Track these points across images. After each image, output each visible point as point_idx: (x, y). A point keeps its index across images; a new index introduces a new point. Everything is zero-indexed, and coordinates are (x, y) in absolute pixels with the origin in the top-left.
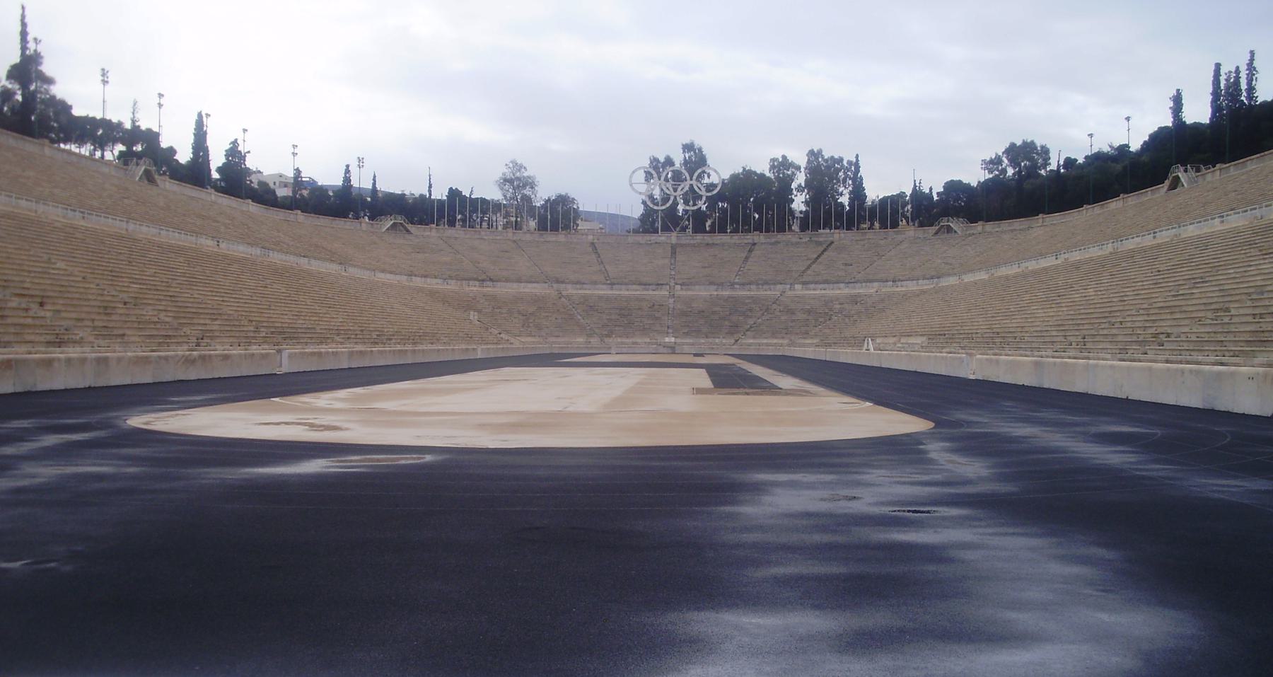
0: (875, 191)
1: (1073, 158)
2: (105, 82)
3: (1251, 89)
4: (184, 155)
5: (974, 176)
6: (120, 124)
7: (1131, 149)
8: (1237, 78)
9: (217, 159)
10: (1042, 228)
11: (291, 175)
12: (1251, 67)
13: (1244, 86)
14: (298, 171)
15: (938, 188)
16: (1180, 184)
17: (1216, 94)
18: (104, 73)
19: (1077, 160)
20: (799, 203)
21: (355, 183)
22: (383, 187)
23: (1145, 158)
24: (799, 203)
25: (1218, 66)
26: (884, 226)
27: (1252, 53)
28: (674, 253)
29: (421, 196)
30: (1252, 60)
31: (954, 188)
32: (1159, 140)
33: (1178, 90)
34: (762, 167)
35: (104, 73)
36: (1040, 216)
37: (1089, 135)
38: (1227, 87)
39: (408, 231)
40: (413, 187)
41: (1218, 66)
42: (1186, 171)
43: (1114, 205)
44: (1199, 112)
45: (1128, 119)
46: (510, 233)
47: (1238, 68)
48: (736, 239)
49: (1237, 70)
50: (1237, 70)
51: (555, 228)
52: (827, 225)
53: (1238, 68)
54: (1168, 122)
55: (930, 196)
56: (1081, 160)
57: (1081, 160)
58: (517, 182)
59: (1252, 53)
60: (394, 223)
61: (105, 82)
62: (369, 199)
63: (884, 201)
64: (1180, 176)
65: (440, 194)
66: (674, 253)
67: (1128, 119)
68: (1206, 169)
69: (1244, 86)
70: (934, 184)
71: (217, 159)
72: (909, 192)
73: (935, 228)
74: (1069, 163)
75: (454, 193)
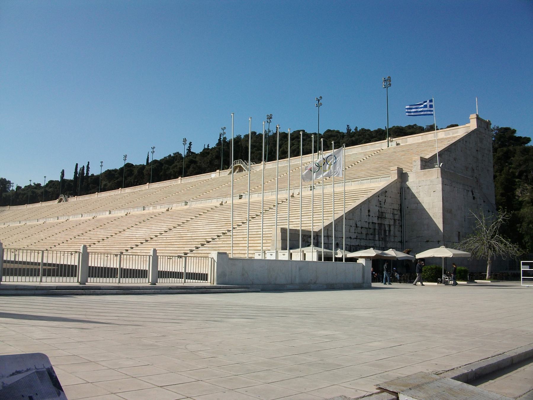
1: (20, 186)
3: (87, 173)
7: (41, 185)
10: (9, 211)
13: (85, 172)
16: (62, 201)
17: (76, 172)
19: (21, 187)
25: (77, 164)
27: (89, 162)
30: (88, 164)
33: (63, 170)
36: (9, 206)
37: (30, 180)
38: (80, 173)
41: (77, 164)
42: (65, 197)
45: (45, 177)
47: (84, 166)
53: (84, 166)
54: (59, 180)
56: (23, 187)
57: (23, 187)
59: (89, 162)
64: (63, 198)
67: (45, 177)
68: (72, 197)
69: (85, 172)
74: (19, 188)
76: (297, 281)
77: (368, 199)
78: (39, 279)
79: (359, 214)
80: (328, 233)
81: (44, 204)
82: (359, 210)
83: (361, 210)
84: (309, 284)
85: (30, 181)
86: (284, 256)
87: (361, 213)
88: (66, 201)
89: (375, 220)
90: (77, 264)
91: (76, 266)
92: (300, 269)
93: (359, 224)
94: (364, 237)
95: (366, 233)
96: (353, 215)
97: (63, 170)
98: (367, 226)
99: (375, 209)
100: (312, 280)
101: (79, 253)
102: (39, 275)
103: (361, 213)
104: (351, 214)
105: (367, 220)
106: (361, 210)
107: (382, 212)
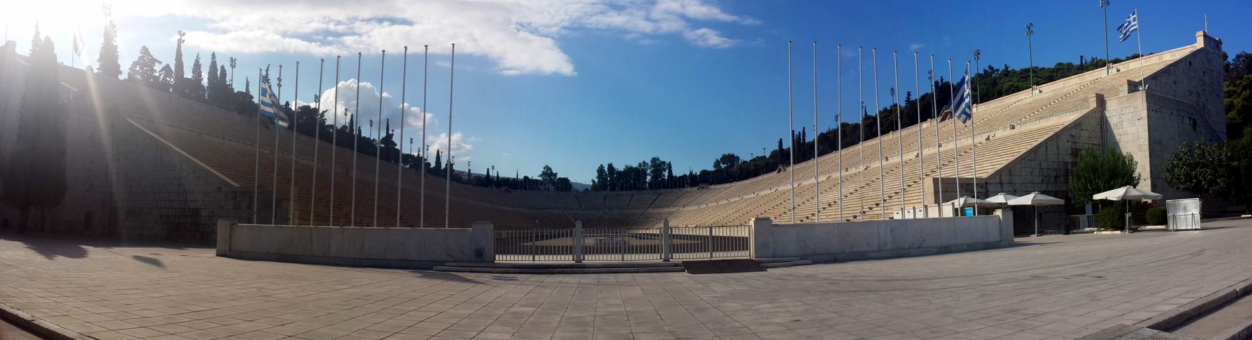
0: (677, 172)
2: (411, 143)
3: (804, 139)
4: (433, 165)
5: (711, 168)
6: (414, 155)
8: (800, 135)
9: (443, 166)
11: (467, 171)
12: (804, 133)
14: (469, 170)
15: (698, 173)
18: (411, 139)
20: (649, 178)
21: (491, 174)
22: (501, 175)
23: (771, 161)
24: (649, 178)
26: (679, 187)
27: (804, 128)
28: (605, 198)
29: (514, 179)
30: (804, 130)
31: (704, 173)
32: (774, 154)
33: (781, 139)
34: (635, 165)
35: (411, 139)
39: (509, 192)
40: (512, 175)
43: (760, 178)
44: (788, 144)
46: (546, 192)
48: (627, 192)
49: (800, 133)
50: (800, 133)
51: (562, 190)
52: (659, 188)
55: (696, 176)
58: (548, 173)
59: (804, 128)
60: (506, 189)
61: (411, 143)
62: (495, 179)
63: (679, 177)
65: (521, 177)
66: (605, 198)
70: (697, 171)
71: (443, 166)
72: (688, 174)
73: (697, 188)
74: (745, 162)
75: (526, 178)
76: (889, 246)
77: (1056, 134)
78: (709, 254)
79: (1044, 152)
80: (1001, 179)
81: (765, 176)
82: (1044, 148)
83: (1046, 147)
84: (910, 248)
85: (752, 154)
86: (933, 213)
87: (1046, 151)
88: (785, 170)
89: (1069, 159)
90: (747, 236)
91: (747, 238)
92: (892, 230)
93: (1044, 165)
94: (1053, 180)
95: (1055, 175)
96: (1035, 154)
97: (781, 139)
98: (1056, 167)
99: (1066, 145)
100: (913, 243)
101: (749, 226)
102: (708, 251)
103: (1046, 151)
104: (1033, 154)
105: (1055, 160)
106: (1046, 147)
107: (1076, 149)
